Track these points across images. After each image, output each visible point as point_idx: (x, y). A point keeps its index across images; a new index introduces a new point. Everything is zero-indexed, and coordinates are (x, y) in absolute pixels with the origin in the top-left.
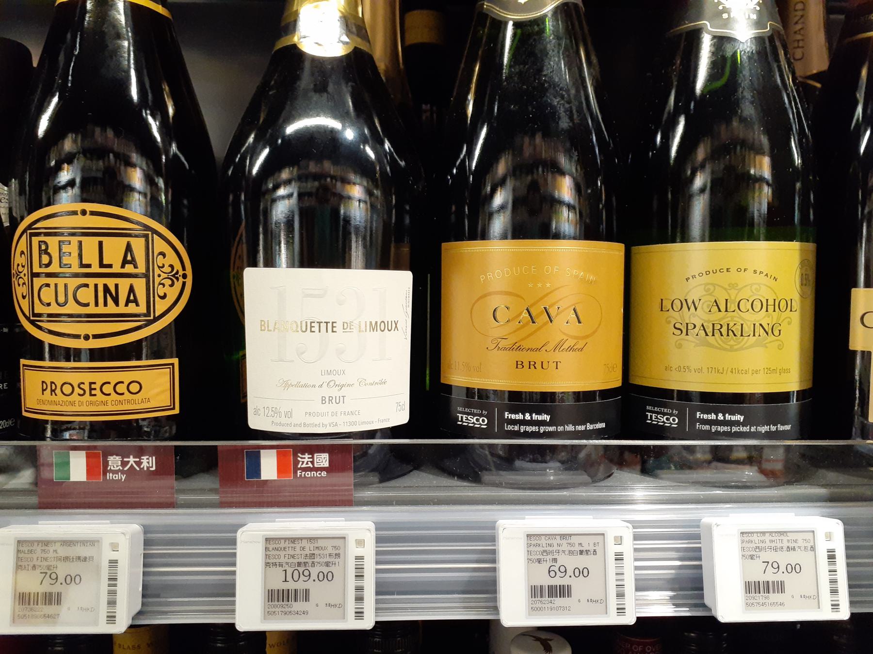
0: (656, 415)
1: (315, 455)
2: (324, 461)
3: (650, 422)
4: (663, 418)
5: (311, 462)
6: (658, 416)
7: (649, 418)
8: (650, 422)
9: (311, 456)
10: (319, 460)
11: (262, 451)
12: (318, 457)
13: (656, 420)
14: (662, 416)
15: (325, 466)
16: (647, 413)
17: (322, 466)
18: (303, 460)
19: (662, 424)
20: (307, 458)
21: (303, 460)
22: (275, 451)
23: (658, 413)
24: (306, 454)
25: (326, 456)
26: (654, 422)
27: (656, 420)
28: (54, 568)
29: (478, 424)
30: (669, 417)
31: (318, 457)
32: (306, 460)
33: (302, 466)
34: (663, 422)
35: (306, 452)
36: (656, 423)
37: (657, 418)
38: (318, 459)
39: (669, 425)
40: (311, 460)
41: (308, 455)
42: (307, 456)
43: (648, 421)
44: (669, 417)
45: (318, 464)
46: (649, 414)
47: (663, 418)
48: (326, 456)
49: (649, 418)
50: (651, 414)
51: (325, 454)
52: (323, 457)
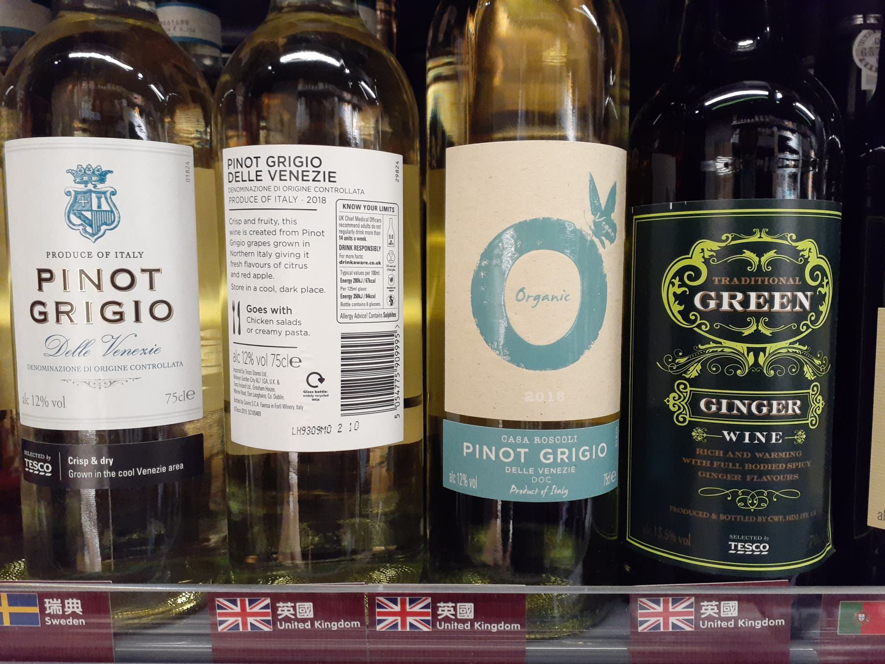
0: (743, 544)
3: (734, 552)
4: (752, 546)
6: (746, 545)
7: (733, 548)
8: (734, 552)
13: (743, 549)
14: (751, 544)
16: (730, 543)
19: (750, 553)
23: (745, 542)
26: (739, 552)
27: (743, 549)
30: (759, 544)
34: (753, 551)
36: (742, 552)
37: (744, 547)
39: (758, 553)
43: (731, 552)
44: (759, 544)
46: (733, 544)
47: (752, 546)
49: (733, 548)
50: (736, 543)
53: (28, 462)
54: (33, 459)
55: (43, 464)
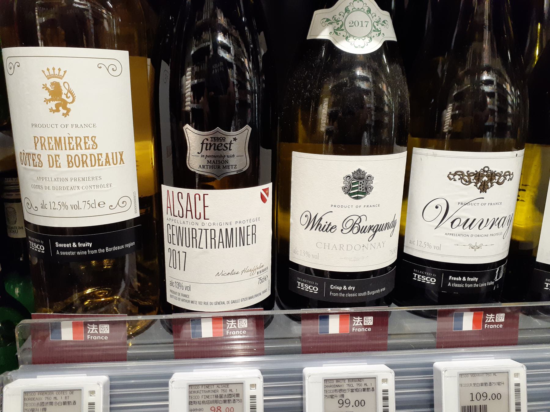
1: (365, 318)
2: (370, 321)
5: (361, 322)
9: (361, 318)
10: (367, 321)
11: (330, 315)
12: (366, 319)
15: (371, 324)
17: (368, 324)
18: (356, 321)
20: (359, 320)
21: (356, 321)
22: (338, 315)
24: (359, 317)
25: (372, 318)
28: (335, 396)
29: (312, 291)
31: (366, 319)
32: (358, 321)
33: (356, 325)
35: (359, 316)
38: (366, 320)
40: (362, 321)
41: (360, 317)
42: (359, 318)
45: (366, 323)
48: (372, 318)
51: (371, 317)
52: (369, 319)
53: (31, 243)
54: (34, 242)
55: (39, 245)
